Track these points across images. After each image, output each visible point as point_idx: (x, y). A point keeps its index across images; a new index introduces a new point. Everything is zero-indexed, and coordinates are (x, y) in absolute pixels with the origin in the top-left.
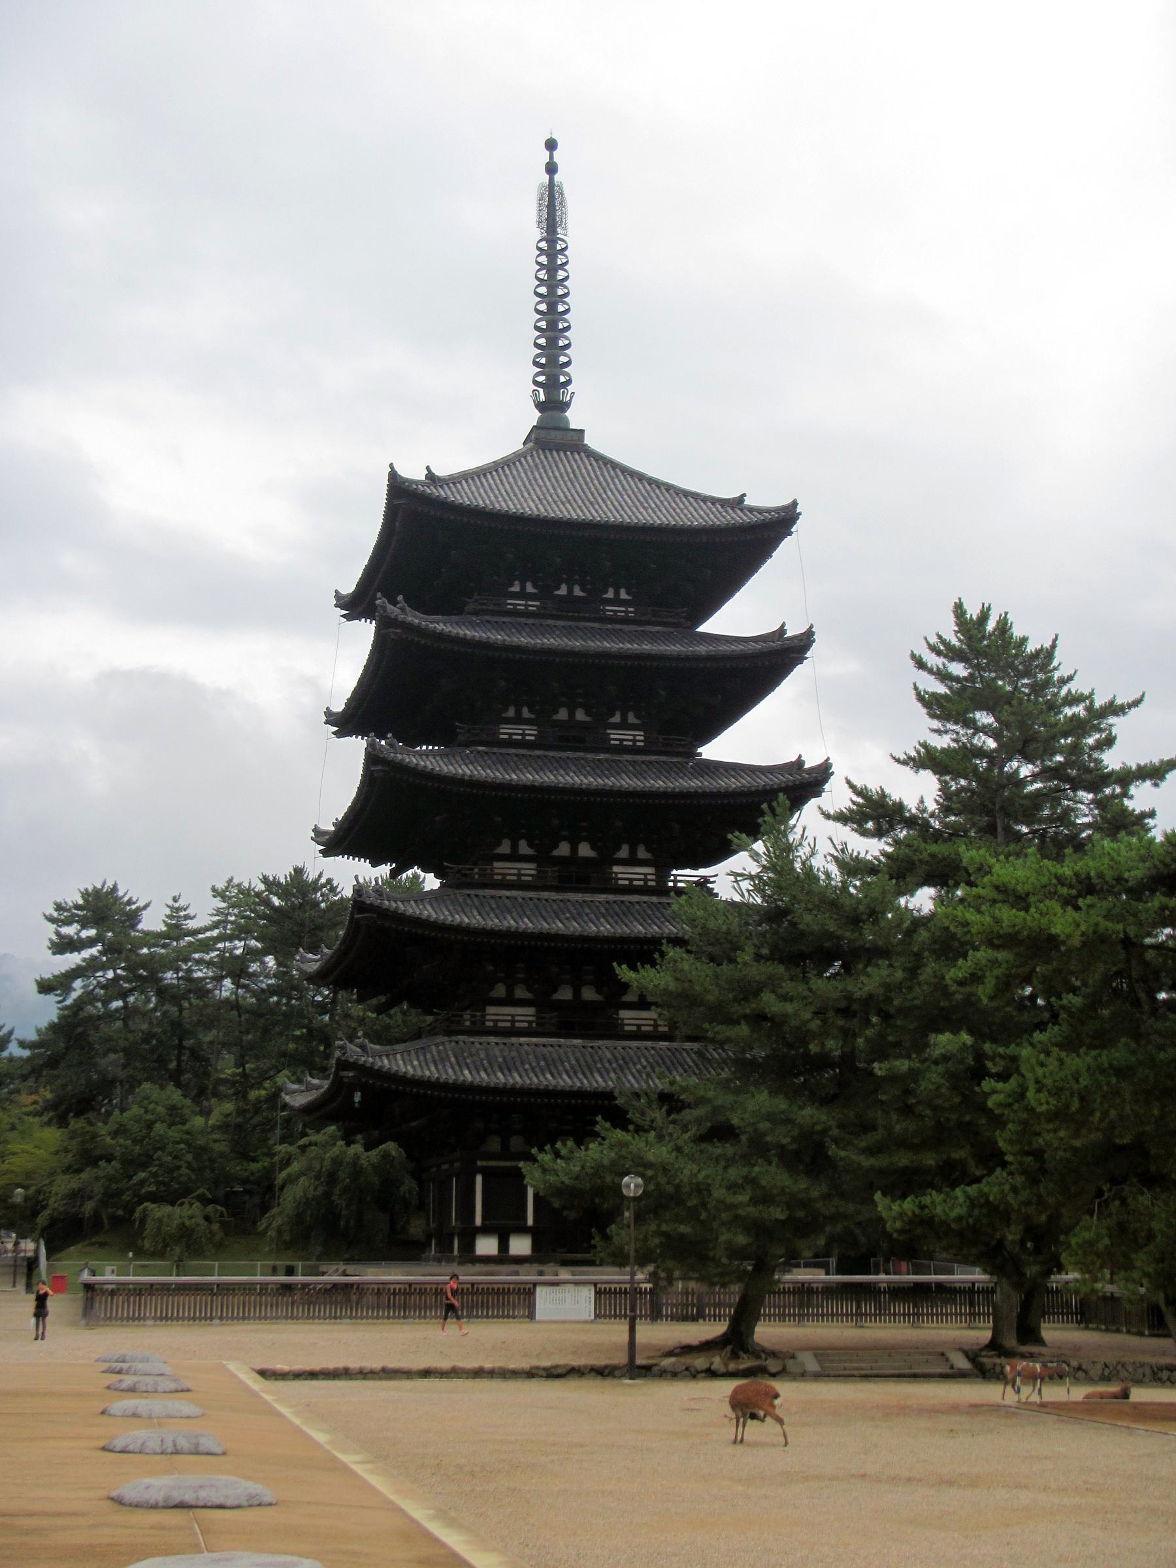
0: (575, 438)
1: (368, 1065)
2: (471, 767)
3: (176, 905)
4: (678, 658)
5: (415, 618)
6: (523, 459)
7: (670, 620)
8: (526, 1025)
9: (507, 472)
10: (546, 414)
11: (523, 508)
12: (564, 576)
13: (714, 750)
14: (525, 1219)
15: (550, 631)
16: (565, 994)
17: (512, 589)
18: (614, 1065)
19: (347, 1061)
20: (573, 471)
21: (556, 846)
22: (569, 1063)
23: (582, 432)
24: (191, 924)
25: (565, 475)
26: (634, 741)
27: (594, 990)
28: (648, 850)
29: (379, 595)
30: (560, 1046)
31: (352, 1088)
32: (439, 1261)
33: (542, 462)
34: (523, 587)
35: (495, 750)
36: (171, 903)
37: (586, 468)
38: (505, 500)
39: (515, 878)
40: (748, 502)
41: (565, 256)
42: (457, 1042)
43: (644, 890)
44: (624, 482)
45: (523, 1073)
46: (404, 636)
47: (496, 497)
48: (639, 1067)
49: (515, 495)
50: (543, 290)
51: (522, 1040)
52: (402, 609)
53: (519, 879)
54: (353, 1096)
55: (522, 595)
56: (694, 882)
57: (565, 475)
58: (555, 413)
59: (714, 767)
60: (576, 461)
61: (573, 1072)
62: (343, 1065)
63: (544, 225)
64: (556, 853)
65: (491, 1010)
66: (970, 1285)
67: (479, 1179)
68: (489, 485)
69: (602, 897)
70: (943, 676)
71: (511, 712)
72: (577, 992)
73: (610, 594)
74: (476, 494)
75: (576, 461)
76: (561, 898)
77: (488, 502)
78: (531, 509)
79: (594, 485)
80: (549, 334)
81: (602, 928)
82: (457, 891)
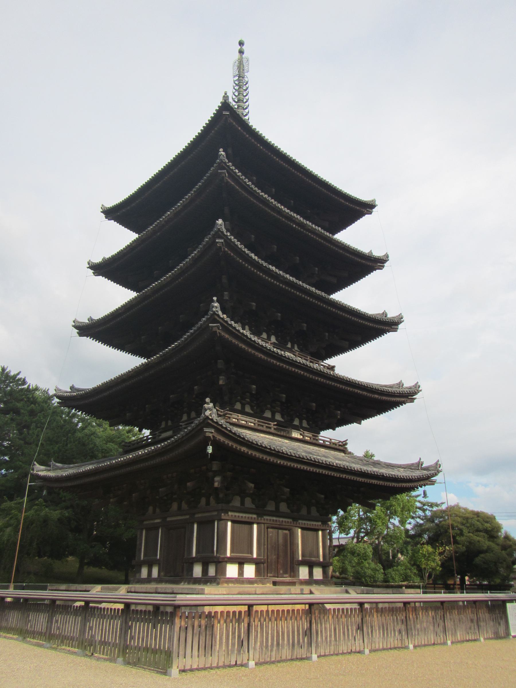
14: (251, 553)
27: (281, 416)
28: (298, 348)
29: (221, 150)
31: (206, 441)
46: (229, 180)
54: (206, 449)
56: (326, 366)
62: (207, 422)
72: (273, 415)
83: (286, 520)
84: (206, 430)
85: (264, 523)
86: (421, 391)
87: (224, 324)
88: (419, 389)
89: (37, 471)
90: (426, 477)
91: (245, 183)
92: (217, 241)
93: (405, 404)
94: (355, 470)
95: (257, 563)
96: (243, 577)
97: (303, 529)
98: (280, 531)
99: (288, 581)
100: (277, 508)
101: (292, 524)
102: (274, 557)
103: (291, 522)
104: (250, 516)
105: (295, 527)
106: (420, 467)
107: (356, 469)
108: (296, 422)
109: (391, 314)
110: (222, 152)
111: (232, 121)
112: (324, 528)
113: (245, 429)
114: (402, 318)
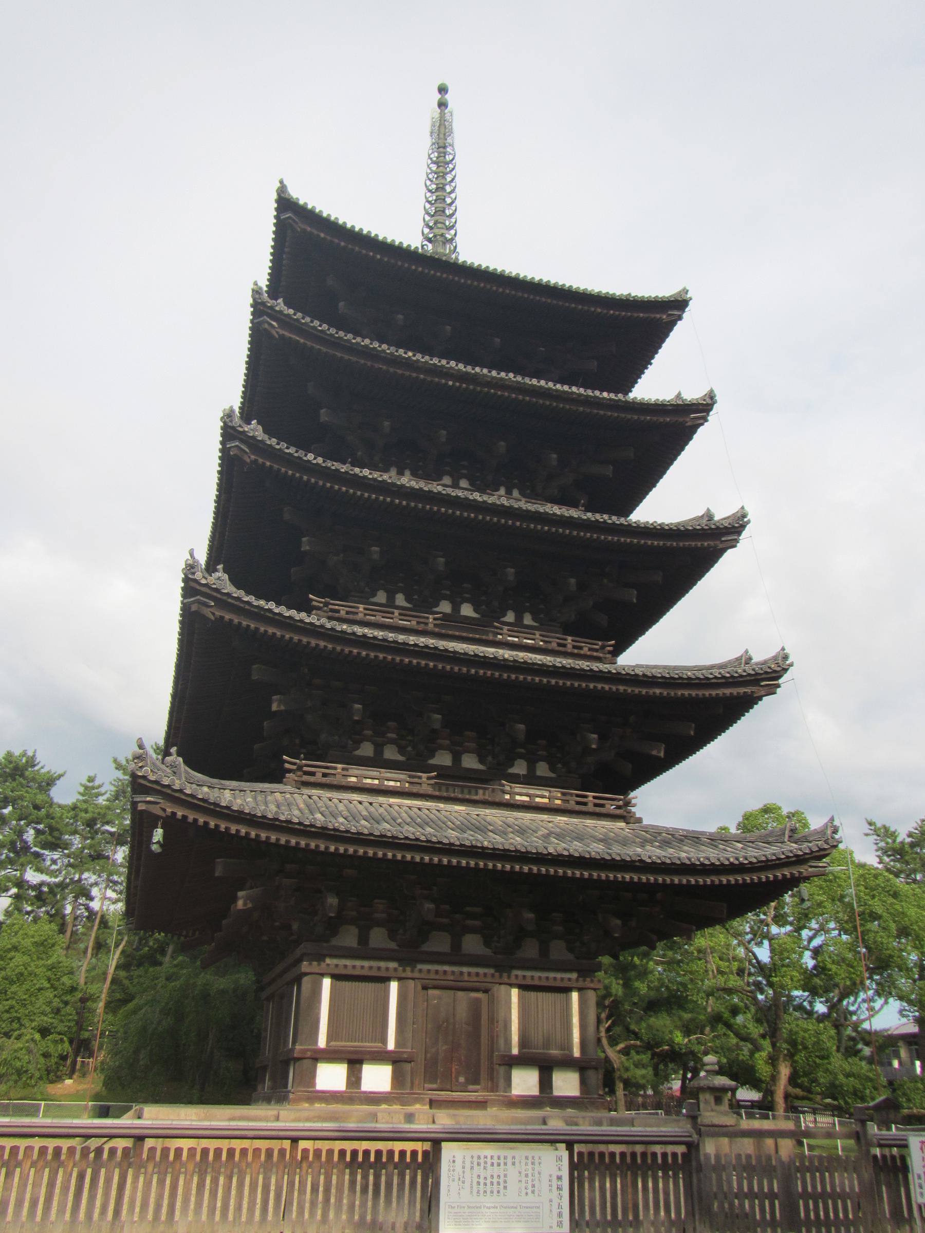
1: (177, 787)
3: (90, 784)
14: (384, 1041)
16: (443, 759)
19: (144, 777)
21: (437, 605)
27: (477, 760)
28: (534, 619)
36: (85, 782)
42: (310, 797)
46: (281, 332)
51: (392, 800)
67: (327, 982)
72: (457, 758)
83: (481, 971)
85: (413, 979)
86: (791, 665)
87: (215, 594)
88: (788, 662)
90: (788, 857)
91: (315, 328)
92: (228, 446)
93: (760, 698)
94: (550, 854)
95: (396, 1060)
96: (360, 1089)
97: (523, 987)
98: (460, 994)
99: (473, 1099)
100: (456, 946)
101: (489, 979)
102: (443, 1048)
103: (485, 975)
104: (383, 964)
105: (497, 986)
106: (787, 836)
107: (551, 850)
108: (519, 768)
109: (722, 513)
111: (303, 226)
112: (580, 984)
113: (353, 793)
114: (744, 516)
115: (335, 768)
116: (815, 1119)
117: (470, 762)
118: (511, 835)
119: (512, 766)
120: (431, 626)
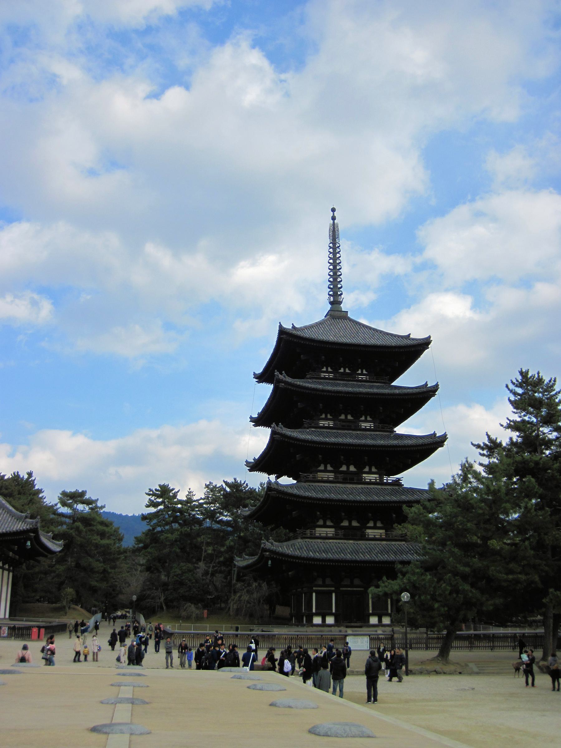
0: (345, 314)
2: (311, 436)
4: (389, 394)
5: (289, 380)
6: (326, 322)
7: (383, 381)
8: (331, 535)
9: (321, 326)
10: (333, 306)
11: (329, 339)
12: (342, 365)
13: (401, 429)
14: (332, 610)
15: (338, 385)
16: (345, 523)
17: (323, 370)
18: (367, 550)
19: (266, 548)
20: (345, 326)
21: (341, 467)
22: (349, 550)
23: (347, 312)
24: (195, 498)
25: (342, 327)
26: (370, 426)
28: (375, 468)
29: (276, 371)
30: (345, 543)
31: (268, 559)
32: (298, 626)
33: (333, 323)
34: (327, 369)
35: (318, 430)
37: (349, 325)
38: (322, 336)
39: (327, 479)
40: (411, 336)
41: (339, 249)
43: (375, 483)
44: (364, 330)
45: (332, 553)
46: (285, 386)
47: (318, 335)
48: (376, 551)
49: (325, 334)
50: (331, 261)
51: (330, 541)
52: (284, 376)
53: (328, 479)
55: (327, 372)
57: (342, 327)
58: (337, 305)
59: (401, 436)
60: (345, 322)
61: (351, 553)
62: (265, 550)
63: (331, 238)
64: (341, 469)
65: (317, 529)
66: (514, 635)
67: (314, 594)
68: (315, 331)
69: (360, 486)
70: (515, 394)
71: (323, 416)
72: (350, 523)
73: (360, 372)
74: (311, 334)
75: (345, 322)
76: (344, 486)
77: (315, 336)
78: (332, 339)
79: (353, 331)
80: (335, 277)
81: (362, 498)
82: (305, 484)
84: (264, 553)
89: (236, 561)
96: (325, 622)
108: (371, 524)
110: (276, 373)
115: (312, 532)
116: (537, 624)
117: (355, 524)
118: (366, 554)
119: (368, 523)
120: (340, 480)
